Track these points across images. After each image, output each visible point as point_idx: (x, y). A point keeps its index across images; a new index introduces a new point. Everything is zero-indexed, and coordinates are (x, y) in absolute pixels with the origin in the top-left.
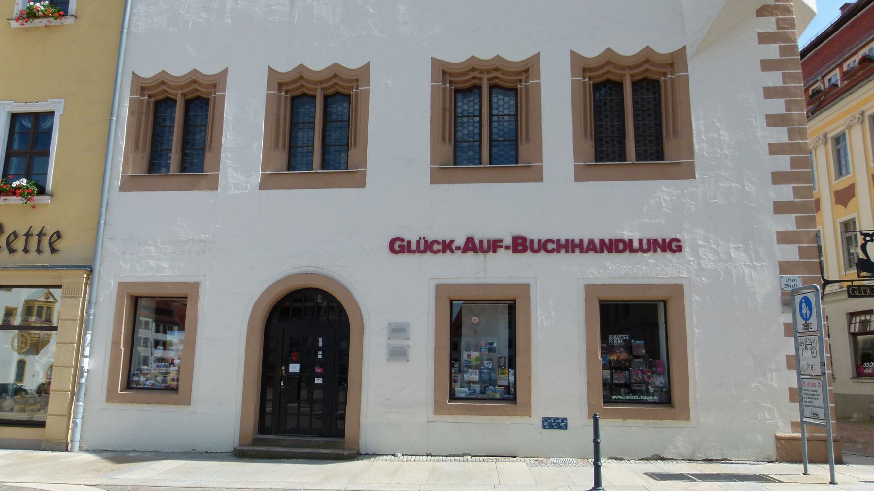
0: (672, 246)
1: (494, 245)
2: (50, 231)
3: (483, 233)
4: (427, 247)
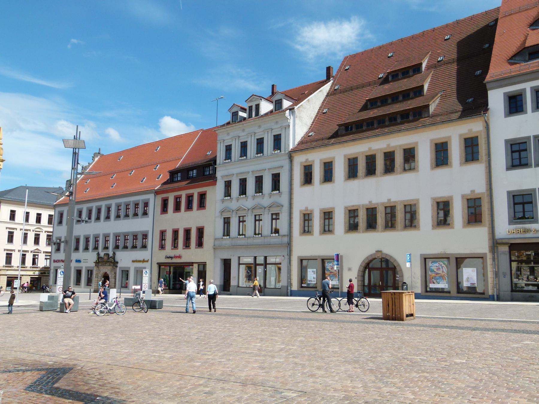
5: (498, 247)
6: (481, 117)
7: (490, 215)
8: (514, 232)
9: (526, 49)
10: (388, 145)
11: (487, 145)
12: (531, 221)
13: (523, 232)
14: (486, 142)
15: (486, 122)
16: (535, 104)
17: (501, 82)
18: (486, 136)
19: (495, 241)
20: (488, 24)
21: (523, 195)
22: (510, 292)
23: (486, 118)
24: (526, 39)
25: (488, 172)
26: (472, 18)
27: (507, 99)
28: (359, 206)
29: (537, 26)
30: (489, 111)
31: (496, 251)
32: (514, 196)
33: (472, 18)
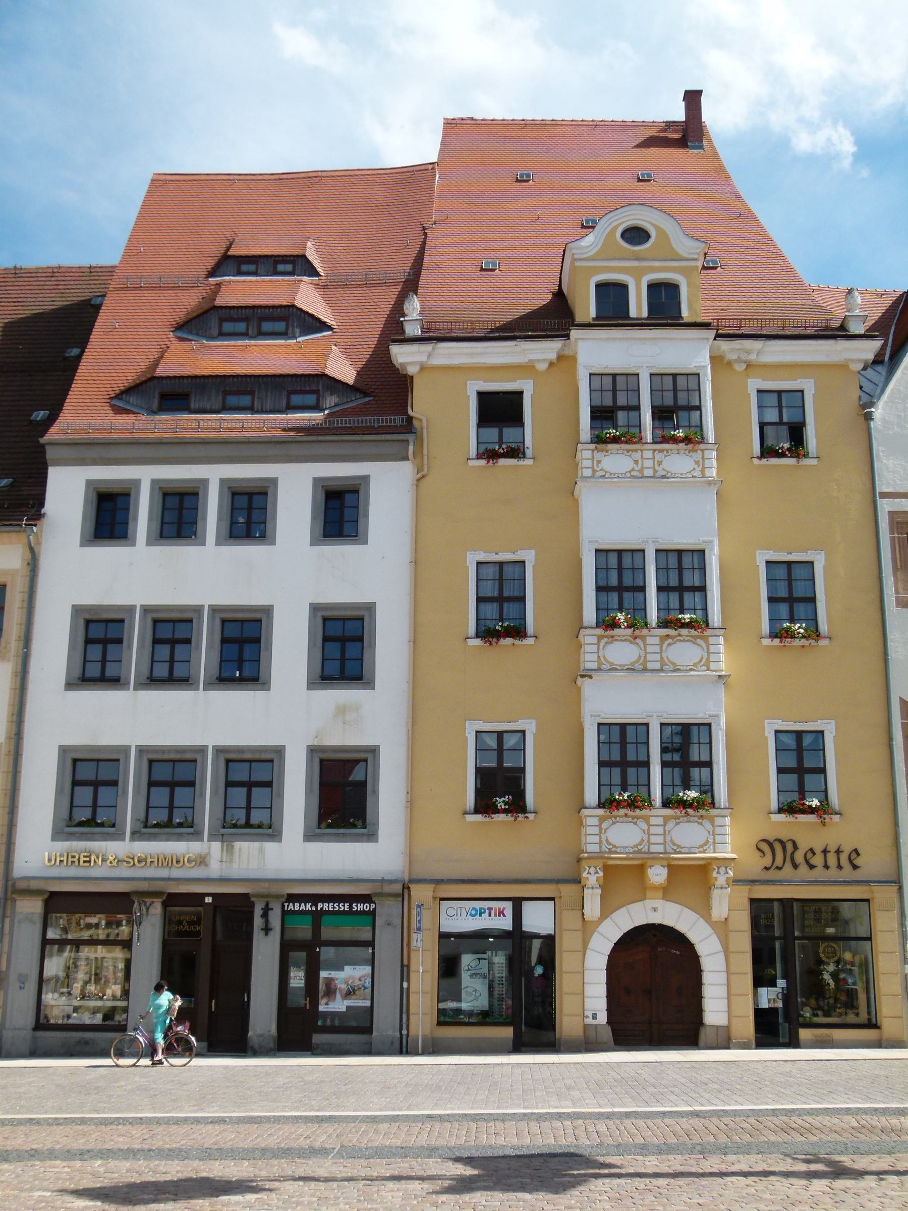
2: (847, 849)
5: (15, 901)
6: (20, 531)
7: (7, 810)
8: (74, 862)
9: (156, 381)
11: (25, 610)
12: (108, 834)
13: (84, 862)
14: (25, 605)
15: (32, 550)
16: (157, 525)
18: (27, 589)
19: (10, 883)
20: (90, 300)
21: (98, 760)
22: (31, 1032)
23: (31, 537)
24: (161, 357)
25: (18, 686)
26: (53, 272)
27: (94, 497)
29: (191, 333)
30: (45, 522)
31: (8, 913)
32: (75, 761)
33: (55, 273)
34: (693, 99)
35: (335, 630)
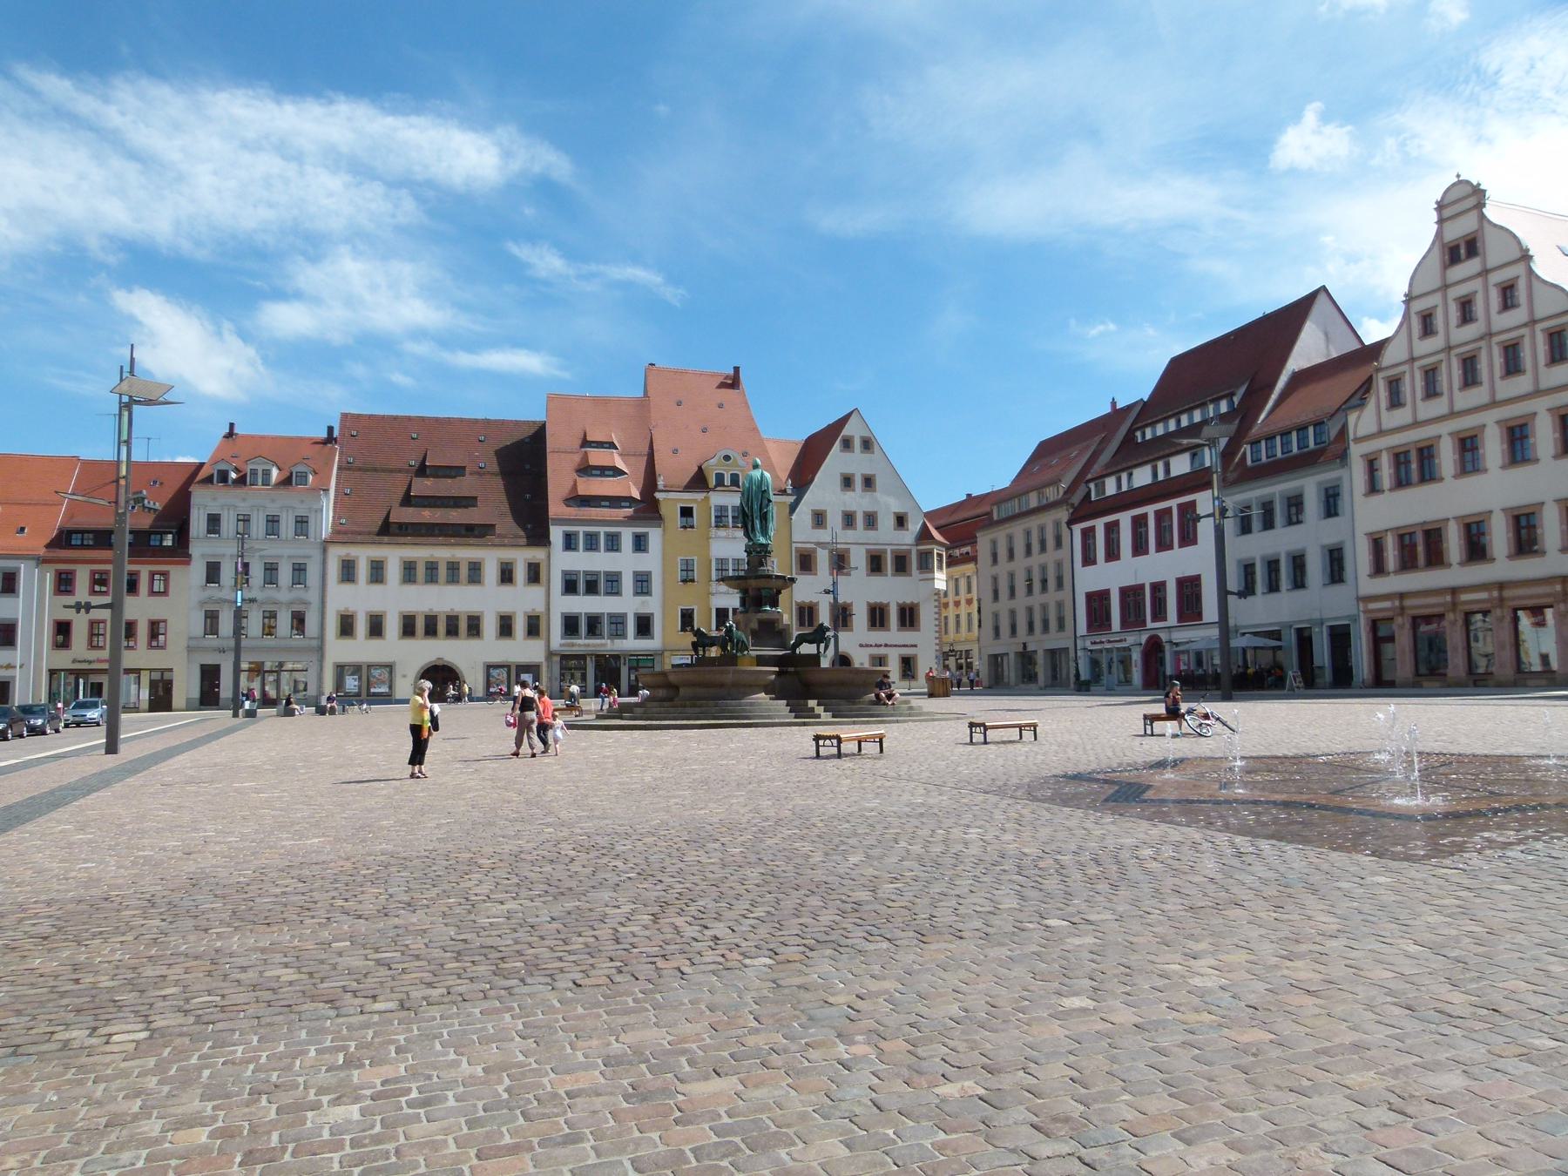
0: (915, 646)
1: (881, 646)
3: (879, 643)
4: (867, 646)
10: (453, 556)
17: (561, 521)
28: (418, 612)
34: (737, 369)
35: (639, 578)
